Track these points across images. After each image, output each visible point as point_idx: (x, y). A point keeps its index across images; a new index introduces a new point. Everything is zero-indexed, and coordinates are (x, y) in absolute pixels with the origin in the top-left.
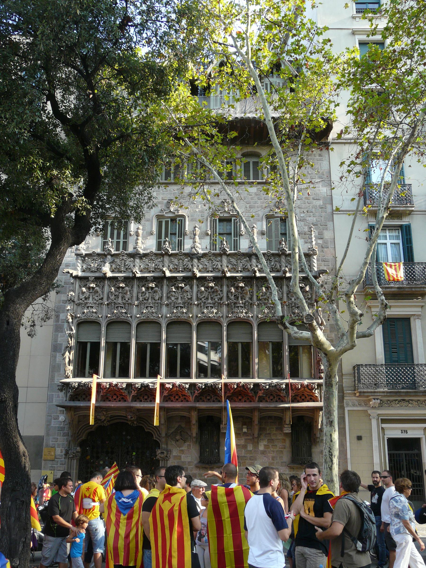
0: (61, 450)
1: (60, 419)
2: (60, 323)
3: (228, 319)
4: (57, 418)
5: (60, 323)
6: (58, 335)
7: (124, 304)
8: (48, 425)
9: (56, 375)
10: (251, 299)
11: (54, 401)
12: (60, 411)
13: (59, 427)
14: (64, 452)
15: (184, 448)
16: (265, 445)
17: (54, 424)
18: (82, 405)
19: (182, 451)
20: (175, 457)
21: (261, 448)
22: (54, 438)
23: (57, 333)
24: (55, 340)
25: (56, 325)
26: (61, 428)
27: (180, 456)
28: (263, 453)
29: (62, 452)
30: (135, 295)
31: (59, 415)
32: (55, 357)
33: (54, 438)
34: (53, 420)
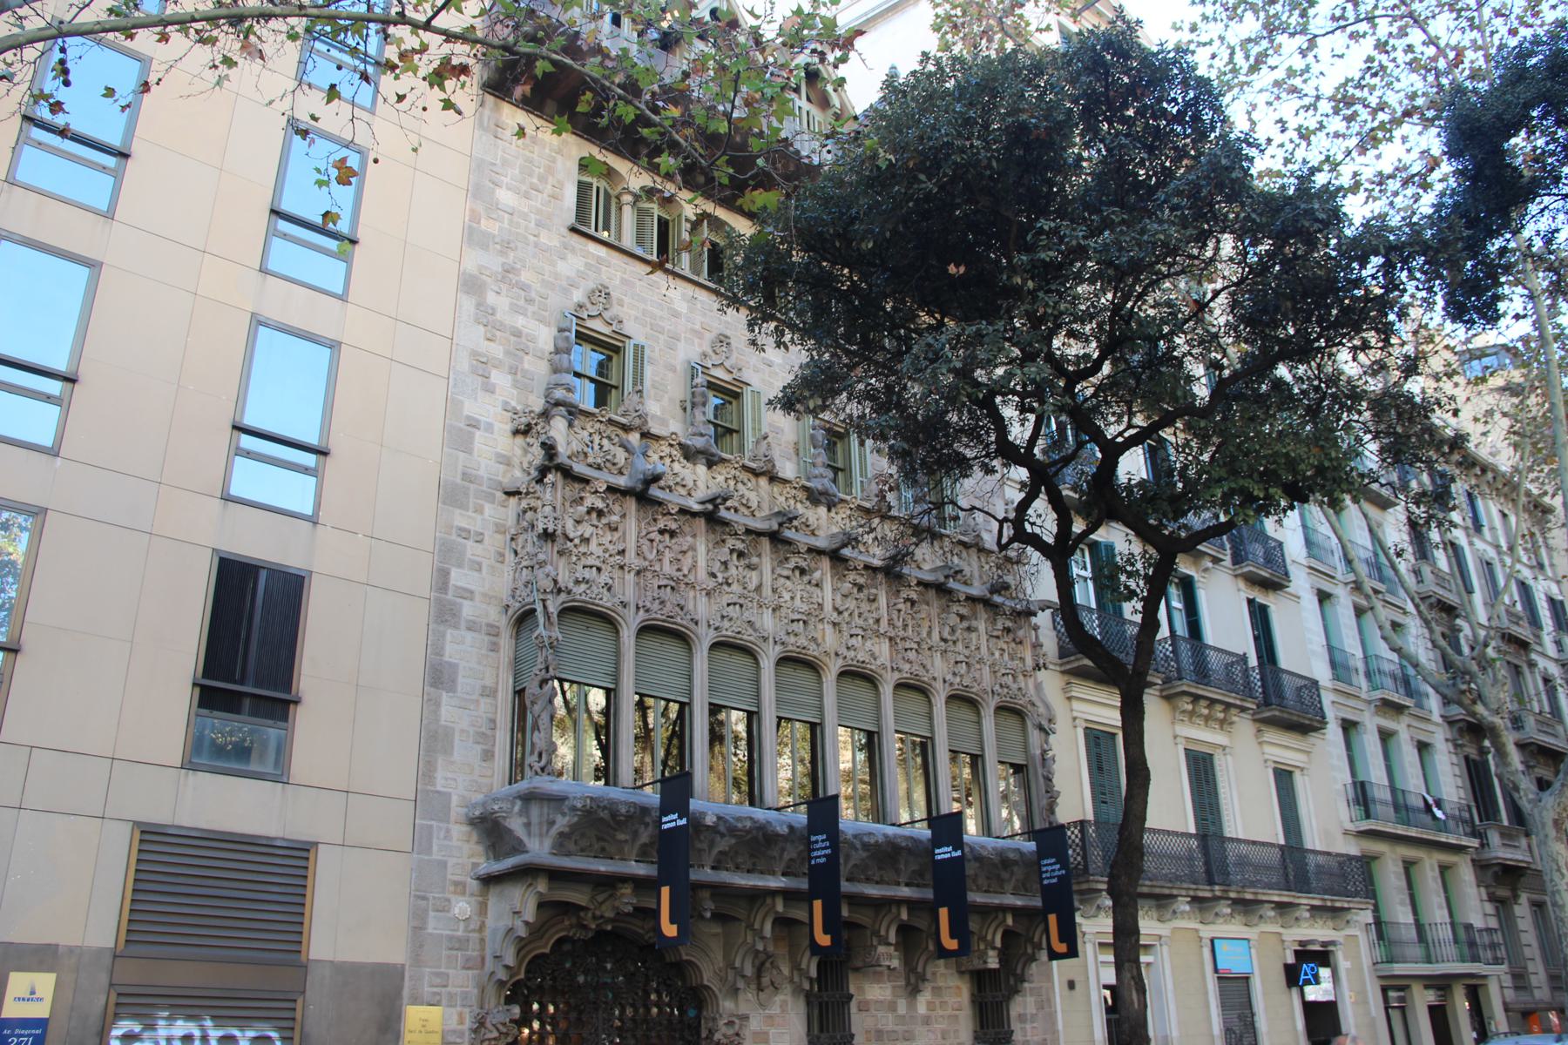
0: (461, 1015)
1: (457, 911)
2: (450, 596)
3: (897, 675)
4: (444, 907)
5: (450, 596)
6: (444, 636)
7: (678, 581)
8: (418, 929)
9: (440, 762)
10: (929, 633)
11: (435, 848)
12: (456, 884)
13: (450, 938)
14: (469, 1023)
15: (775, 1010)
16: (929, 1003)
17: (434, 926)
18: (602, 869)
19: (770, 1017)
20: (755, 1033)
21: (922, 1008)
22: (438, 975)
23: (442, 628)
24: (435, 648)
25: (439, 601)
26: (459, 939)
27: (766, 1033)
28: (927, 1021)
29: (461, 1022)
30: (702, 563)
31: (453, 898)
32: (438, 704)
33: (438, 975)
34: (432, 914)
